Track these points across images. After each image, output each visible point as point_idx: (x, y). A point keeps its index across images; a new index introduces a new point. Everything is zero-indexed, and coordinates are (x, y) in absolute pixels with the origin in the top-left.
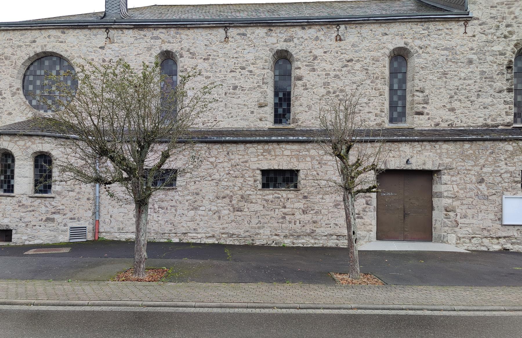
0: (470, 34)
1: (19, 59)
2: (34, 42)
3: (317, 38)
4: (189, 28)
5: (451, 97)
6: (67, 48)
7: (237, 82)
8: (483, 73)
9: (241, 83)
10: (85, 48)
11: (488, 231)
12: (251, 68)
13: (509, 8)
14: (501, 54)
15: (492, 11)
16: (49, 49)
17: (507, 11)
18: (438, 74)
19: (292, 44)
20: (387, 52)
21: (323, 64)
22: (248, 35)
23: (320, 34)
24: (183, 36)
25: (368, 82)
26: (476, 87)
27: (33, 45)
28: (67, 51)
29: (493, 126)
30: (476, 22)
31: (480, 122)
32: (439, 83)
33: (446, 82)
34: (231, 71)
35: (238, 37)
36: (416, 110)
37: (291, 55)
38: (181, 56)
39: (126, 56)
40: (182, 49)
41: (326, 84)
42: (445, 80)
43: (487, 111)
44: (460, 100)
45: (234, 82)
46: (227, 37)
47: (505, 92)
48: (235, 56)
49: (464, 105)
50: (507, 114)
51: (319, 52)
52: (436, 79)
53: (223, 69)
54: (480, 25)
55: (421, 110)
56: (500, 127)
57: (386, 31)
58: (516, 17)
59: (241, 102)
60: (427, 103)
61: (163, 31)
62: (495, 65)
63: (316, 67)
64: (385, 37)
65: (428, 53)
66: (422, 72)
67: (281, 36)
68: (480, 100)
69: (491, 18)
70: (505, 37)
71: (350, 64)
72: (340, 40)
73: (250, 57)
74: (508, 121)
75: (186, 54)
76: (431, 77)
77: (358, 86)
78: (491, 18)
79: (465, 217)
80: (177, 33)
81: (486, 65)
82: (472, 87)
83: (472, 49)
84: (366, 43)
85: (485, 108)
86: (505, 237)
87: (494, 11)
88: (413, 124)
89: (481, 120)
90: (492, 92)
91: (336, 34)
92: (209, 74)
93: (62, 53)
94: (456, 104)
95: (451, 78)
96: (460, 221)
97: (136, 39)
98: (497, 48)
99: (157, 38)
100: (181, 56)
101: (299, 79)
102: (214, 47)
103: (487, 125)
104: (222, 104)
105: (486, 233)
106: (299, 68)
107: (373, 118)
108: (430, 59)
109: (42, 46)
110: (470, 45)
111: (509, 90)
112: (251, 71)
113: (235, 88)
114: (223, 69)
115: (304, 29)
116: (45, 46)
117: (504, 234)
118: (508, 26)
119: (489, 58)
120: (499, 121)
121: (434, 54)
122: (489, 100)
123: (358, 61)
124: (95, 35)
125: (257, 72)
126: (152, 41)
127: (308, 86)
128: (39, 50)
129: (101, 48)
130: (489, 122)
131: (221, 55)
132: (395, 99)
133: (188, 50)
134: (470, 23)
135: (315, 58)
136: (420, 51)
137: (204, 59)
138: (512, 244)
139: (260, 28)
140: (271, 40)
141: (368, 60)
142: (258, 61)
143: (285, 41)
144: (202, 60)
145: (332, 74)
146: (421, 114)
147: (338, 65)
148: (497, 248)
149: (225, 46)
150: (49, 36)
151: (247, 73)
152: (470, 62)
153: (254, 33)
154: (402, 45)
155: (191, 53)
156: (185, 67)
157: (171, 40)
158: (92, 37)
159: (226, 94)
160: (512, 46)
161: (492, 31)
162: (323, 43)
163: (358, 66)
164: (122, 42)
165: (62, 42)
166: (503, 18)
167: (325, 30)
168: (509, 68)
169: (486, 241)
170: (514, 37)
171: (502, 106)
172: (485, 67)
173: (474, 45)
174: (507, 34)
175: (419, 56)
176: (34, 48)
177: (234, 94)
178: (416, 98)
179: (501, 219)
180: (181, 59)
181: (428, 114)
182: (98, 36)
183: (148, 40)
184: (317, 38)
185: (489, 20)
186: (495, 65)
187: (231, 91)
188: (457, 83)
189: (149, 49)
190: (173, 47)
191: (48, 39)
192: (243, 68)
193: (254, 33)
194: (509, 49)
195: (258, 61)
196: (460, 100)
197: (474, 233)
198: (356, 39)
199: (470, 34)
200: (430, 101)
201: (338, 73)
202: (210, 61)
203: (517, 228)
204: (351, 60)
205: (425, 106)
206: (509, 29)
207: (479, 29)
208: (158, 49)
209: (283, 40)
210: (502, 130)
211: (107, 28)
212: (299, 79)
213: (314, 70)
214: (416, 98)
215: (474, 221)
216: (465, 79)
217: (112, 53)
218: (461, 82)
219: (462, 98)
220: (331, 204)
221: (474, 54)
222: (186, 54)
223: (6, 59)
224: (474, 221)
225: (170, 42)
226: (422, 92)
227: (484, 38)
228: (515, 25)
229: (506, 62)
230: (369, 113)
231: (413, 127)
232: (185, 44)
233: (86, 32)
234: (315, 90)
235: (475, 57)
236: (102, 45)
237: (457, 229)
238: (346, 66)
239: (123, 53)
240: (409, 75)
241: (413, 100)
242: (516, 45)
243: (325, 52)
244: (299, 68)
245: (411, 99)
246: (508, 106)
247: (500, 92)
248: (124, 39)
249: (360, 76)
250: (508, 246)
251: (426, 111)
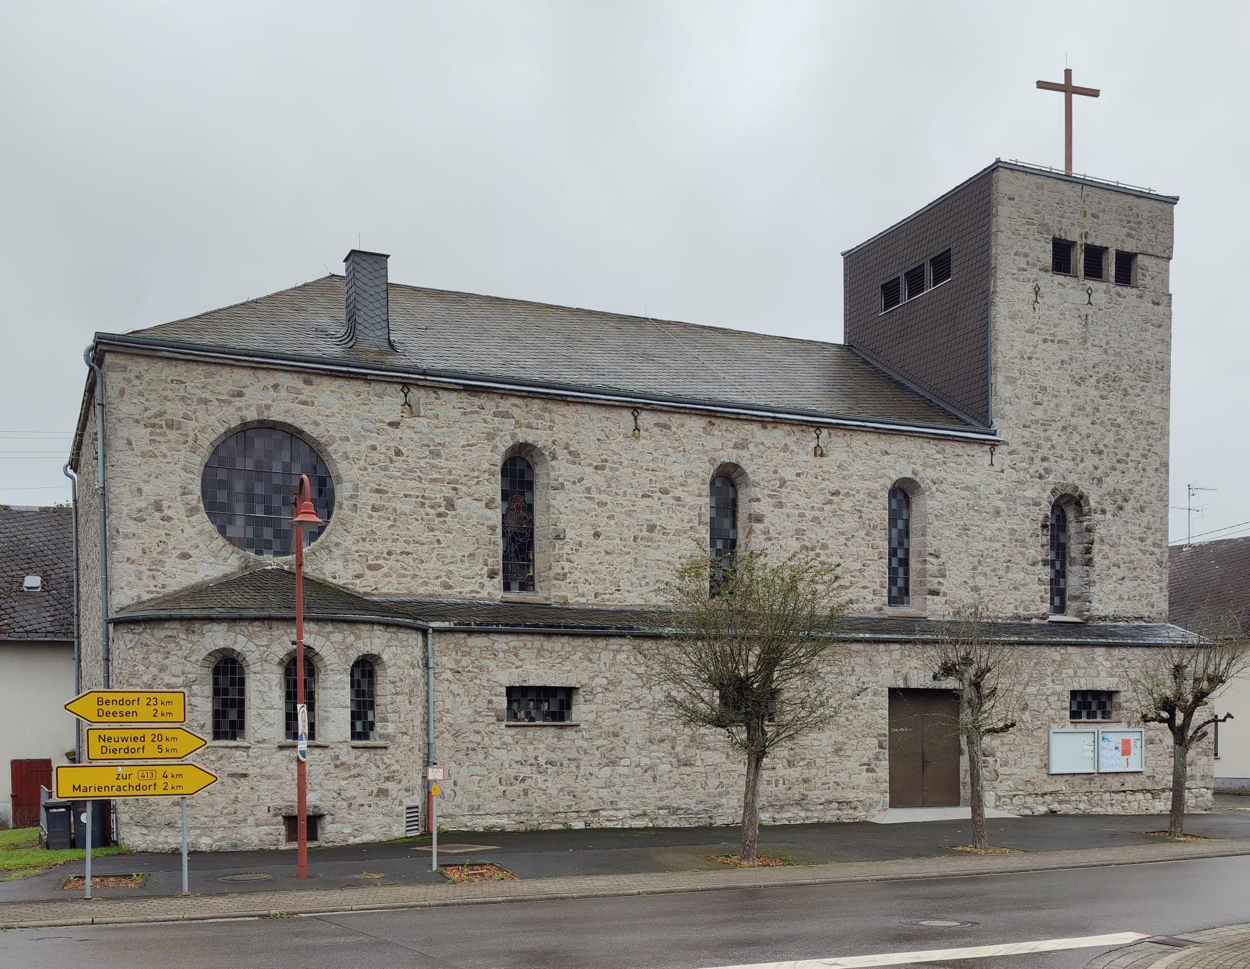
0: (997, 467)
1: (202, 430)
2: (240, 394)
3: (785, 448)
4: (568, 403)
5: (974, 569)
6: (318, 418)
7: (654, 517)
8: (1013, 531)
9: (660, 519)
10: (356, 422)
11: (1033, 784)
12: (678, 492)
13: (1045, 431)
14: (1037, 504)
15: (1025, 434)
16: (276, 415)
17: (1042, 434)
18: (956, 529)
19: (745, 453)
20: (889, 484)
21: (795, 496)
22: (674, 429)
23: (790, 441)
24: (556, 417)
25: (862, 533)
26: (1005, 554)
27: (238, 402)
28: (317, 424)
29: (1025, 619)
30: (1004, 448)
31: (1010, 611)
32: (958, 543)
33: (967, 543)
34: (644, 496)
35: (657, 429)
36: (929, 586)
37: (743, 473)
38: (554, 458)
39: (443, 445)
40: (554, 442)
41: (800, 533)
42: (966, 539)
43: (1018, 595)
44: (985, 574)
45: (649, 517)
46: (637, 428)
47: (1040, 566)
48: (651, 466)
49: (990, 582)
50: (1042, 600)
51: (788, 473)
52: (953, 536)
53: (629, 491)
54: (1010, 453)
55: (936, 587)
56: (1034, 621)
57: (887, 448)
58: (1053, 446)
59: (663, 557)
60: (944, 576)
61: (519, 402)
62: (1027, 520)
63: (784, 501)
64: (886, 458)
65: (943, 492)
66: (936, 523)
67: (728, 436)
68: (1010, 575)
69: (1024, 443)
70: (1041, 477)
71: (835, 499)
72: (822, 455)
73: (677, 471)
74: (1044, 610)
75: (562, 454)
76: (947, 533)
77: (848, 539)
78: (1024, 443)
79: (1006, 764)
80: (544, 410)
81: (1016, 520)
82: (1000, 554)
83: (999, 492)
84: (857, 466)
85: (1015, 588)
86: (1051, 793)
87: (1027, 434)
88: (924, 610)
89: (1011, 607)
90: (1024, 564)
91: (814, 444)
92: (603, 497)
93: (306, 429)
94: (980, 581)
95: (973, 537)
96: (1001, 770)
97: (465, 414)
98: (1031, 493)
99: (506, 415)
100: (554, 458)
101: (759, 519)
102: (614, 446)
103: (1018, 617)
104: (629, 558)
105: (1030, 789)
106: (758, 500)
107: (870, 597)
108: (946, 502)
109: (259, 407)
110: (997, 486)
111: (1045, 562)
112: (678, 499)
113: (651, 528)
114: (629, 491)
115: (765, 428)
116: (268, 407)
117: (1051, 789)
118: (1044, 459)
119: (1021, 509)
120: (1033, 611)
121: (952, 494)
122: (1019, 577)
123: (847, 495)
124: (380, 396)
125: (689, 500)
126: (496, 419)
127: (772, 534)
128: (251, 415)
129: (391, 424)
130: (1021, 612)
131: (626, 463)
132: (895, 564)
133: (567, 447)
134: (998, 449)
135: (783, 483)
136: (934, 488)
137: (596, 468)
138: (1060, 802)
139: (694, 418)
140: (713, 442)
141: (861, 496)
142: (690, 481)
143: (736, 446)
144: (591, 469)
145: (809, 514)
146: (935, 593)
147: (817, 500)
148: (1042, 809)
149: (634, 444)
150: (276, 387)
151: (671, 501)
152: (997, 513)
153: (683, 426)
154: (910, 475)
155: (570, 453)
156: (561, 480)
157: (534, 422)
158: (374, 399)
159: (635, 539)
160: (1048, 493)
161: (1025, 465)
162: (796, 458)
163: (847, 504)
164: (437, 417)
165: (305, 403)
166: (1038, 446)
167: (798, 434)
168: (1044, 526)
169: (1030, 800)
170: (1051, 479)
171: (1036, 587)
172: (1014, 523)
173: (1002, 485)
174: (1042, 472)
175: (932, 496)
176: (240, 409)
177: (651, 540)
178: (928, 566)
179: (1047, 766)
180: (553, 463)
181: (945, 594)
182: (386, 398)
183: (488, 418)
184: (785, 448)
185: (1021, 448)
186: (1027, 520)
187: (645, 533)
188: (983, 546)
189: (490, 437)
190: (538, 437)
191: (272, 393)
192: (665, 491)
193: (683, 426)
194: (1045, 496)
195: (690, 481)
196: (985, 574)
197: (1017, 789)
198: (844, 456)
199: (997, 467)
200: (947, 573)
201: (817, 513)
202: (607, 471)
203: (1066, 778)
204: (836, 493)
205: (941, 580)
206: (1045, 464)
207: (1008, 460)
208: (508, 438)
209: (731, 444)
210: (1037, 625)
211: (405, 385)
212: (759, 519)
213: (780, 505)
214: (928, 566)
215: (1015, 770)
216: (991, 540)
217: (416, 437)
218: (987, 544)
219: (988, 570)
220: (831, 749)
221: (1002, 500)
222: (562, 454)
223: (170, 425)
224: (1015, 770)
225: (530, 426)
226: (937, 557)
227: (1015, 476)
228: (1052, 459)
229: (1041, 518)
230: (865, 587)
231: (925, 615)
232: (561, 435)
233: (360, 386)
234: (783, 543)
235: (1002, 505)
236: (395, 417)
237: (996, 784)
238: (830, 502)
239: (437, 440)
240: (915, 525)
241: (924, 569)
242: (1053, 492)
243: (798, 475)
244: (758, 500)
245: (920, 566)
246: (1043, 587)
247: (1034, 564)
248: (439, 410)
249: (851, 523)
250: (1055, 806)
251: (943, 589)
